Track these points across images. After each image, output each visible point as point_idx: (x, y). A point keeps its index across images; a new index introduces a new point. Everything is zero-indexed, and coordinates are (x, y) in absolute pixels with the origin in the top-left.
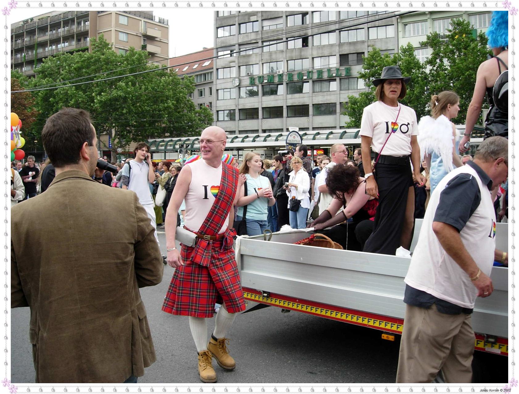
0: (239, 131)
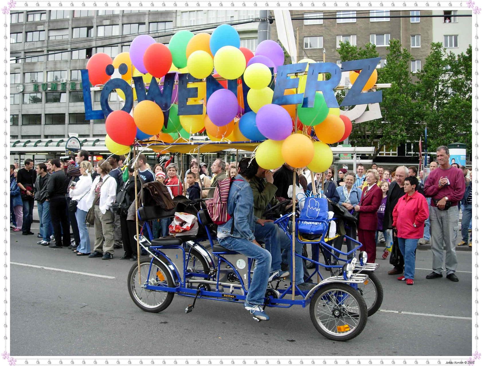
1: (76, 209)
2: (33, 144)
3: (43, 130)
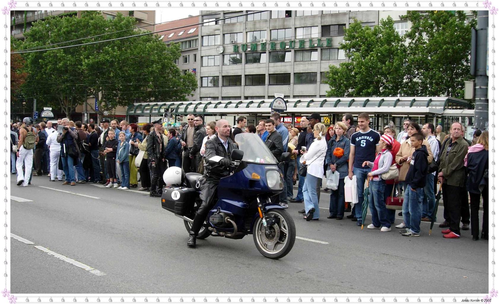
0: (245, 97)
1: (305, 173)
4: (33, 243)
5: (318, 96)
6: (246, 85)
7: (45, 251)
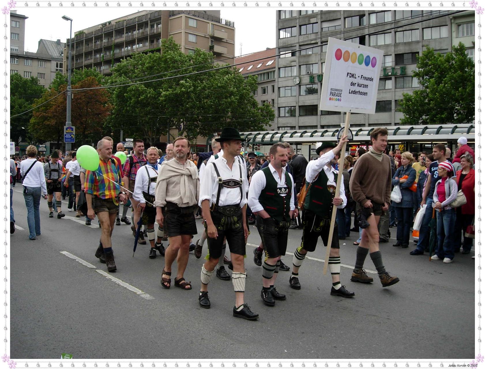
2: (331, 133)
3: (393, 116)
4: (95, 267)
5: (367, 124)
6: (300, 116)
7: (104, 275)
